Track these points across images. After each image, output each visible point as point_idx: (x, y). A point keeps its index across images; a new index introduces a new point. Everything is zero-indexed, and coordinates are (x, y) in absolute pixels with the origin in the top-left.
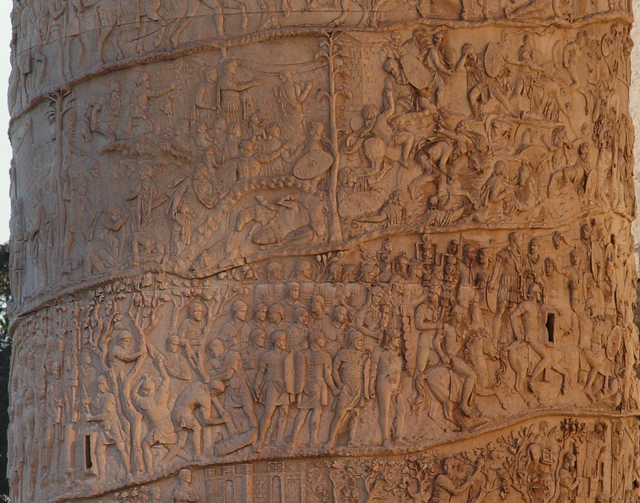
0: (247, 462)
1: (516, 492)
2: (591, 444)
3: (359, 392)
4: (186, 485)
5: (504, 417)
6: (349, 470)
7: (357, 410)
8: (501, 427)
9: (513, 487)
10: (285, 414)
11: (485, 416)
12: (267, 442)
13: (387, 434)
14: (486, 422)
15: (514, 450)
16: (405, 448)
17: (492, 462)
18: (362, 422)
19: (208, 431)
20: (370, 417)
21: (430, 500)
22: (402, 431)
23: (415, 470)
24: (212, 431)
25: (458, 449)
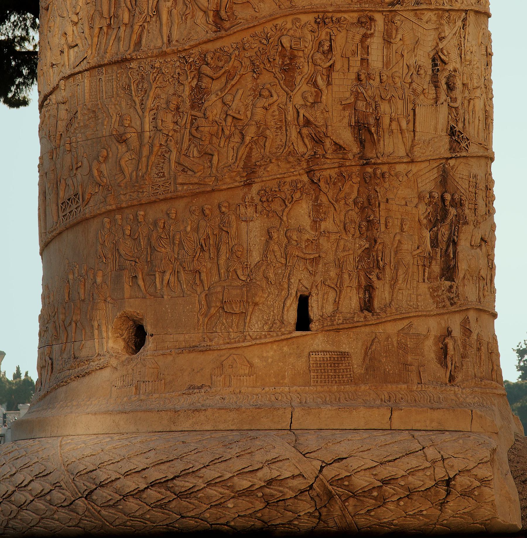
0: (86, 70)
1: (268, 72)
2: (351, 32)
3: (146, 11)
4: (63, 91)
5: (256, 17)
6: (141, 68)
7: (146, 24)
8: (252, 25)
9: (266, 69)
10: (104, 33)
11: (240, 19)
12: (96, 55)
13: (165, 39)
14: (241, 22)
15: (265, 42)
16: (176, 48)
17: (246, 52)
18: (149, 33)
19: (71, 51)
20: (154, 28)
21: (197, 84)
22: (175, 36)
23: (184, 63)
24: (74, 51)
25: (218, 44)
